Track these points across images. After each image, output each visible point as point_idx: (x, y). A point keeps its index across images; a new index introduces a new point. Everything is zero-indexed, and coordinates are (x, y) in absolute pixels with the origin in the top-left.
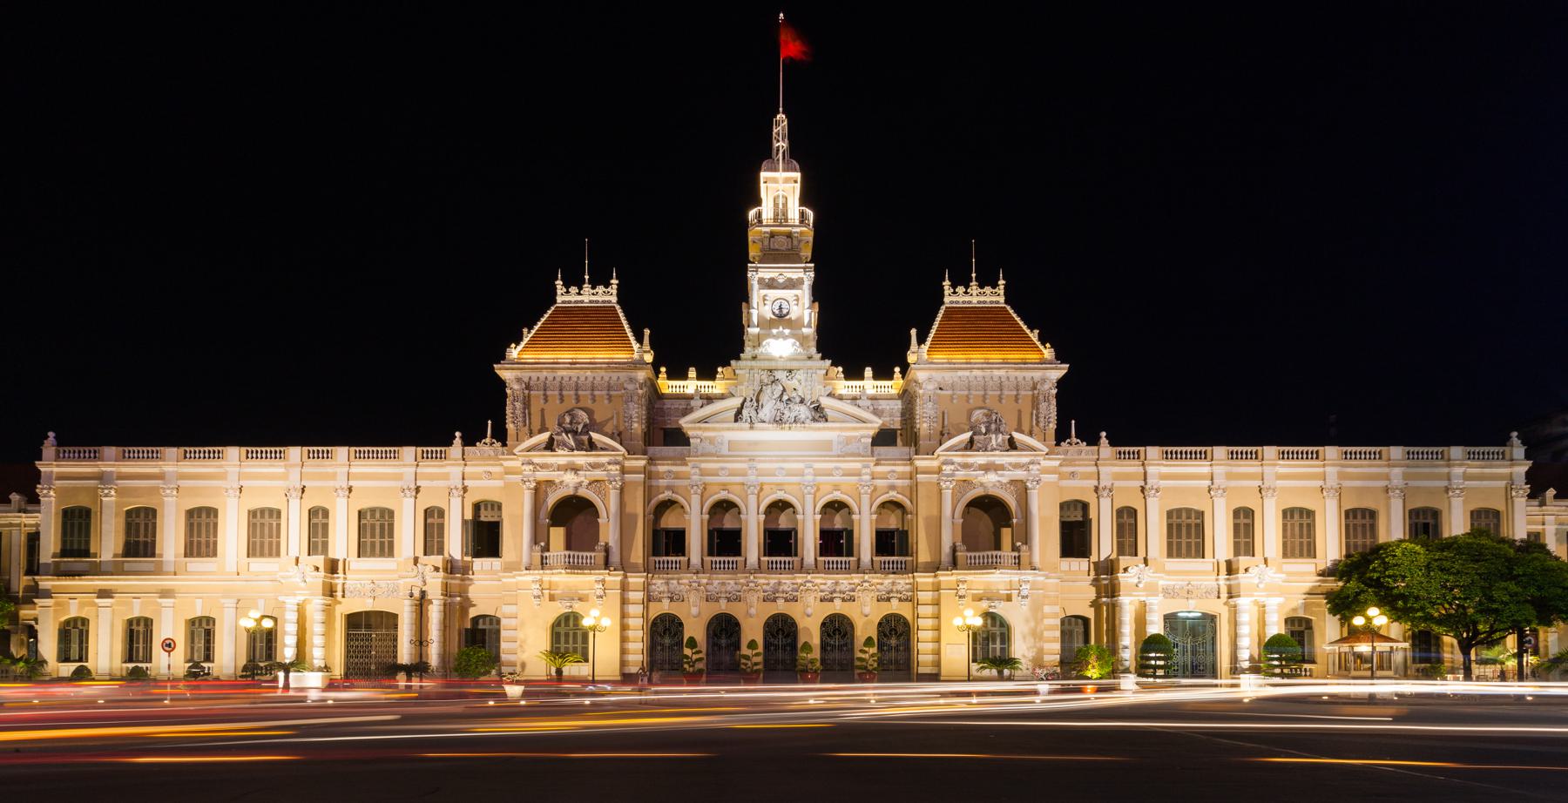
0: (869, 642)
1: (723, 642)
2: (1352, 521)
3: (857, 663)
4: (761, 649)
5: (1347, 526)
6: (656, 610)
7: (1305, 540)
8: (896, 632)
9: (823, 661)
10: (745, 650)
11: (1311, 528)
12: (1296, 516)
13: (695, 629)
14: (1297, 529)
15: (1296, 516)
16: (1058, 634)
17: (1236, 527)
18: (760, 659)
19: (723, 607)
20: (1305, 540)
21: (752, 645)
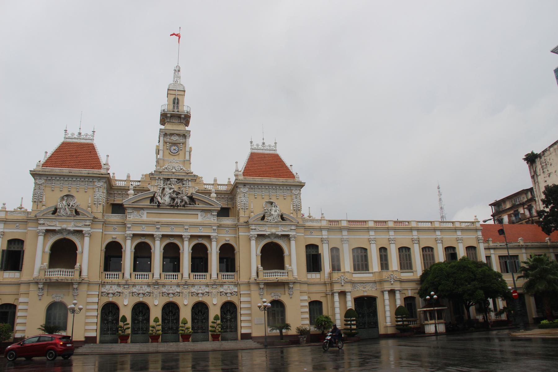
0: (216, 318)
1: (141, 318)
2: (425, 253)
3: (210, 329)
4: (160, 322)
5: (423, 255)
6: (105, 300)
7: (408, 262)
8: (229, 309)
9: (193, 328)
10: (152, 323)
11: (409, 257)
12: (404, 250)
13: (126, 312)
14: (405, 257)
15: (404, 250)
16: (307, 310)
17: (381, 256)
18: (160, 328)
19: (141, 299)
20: (408, 262)
21: (156, 320)
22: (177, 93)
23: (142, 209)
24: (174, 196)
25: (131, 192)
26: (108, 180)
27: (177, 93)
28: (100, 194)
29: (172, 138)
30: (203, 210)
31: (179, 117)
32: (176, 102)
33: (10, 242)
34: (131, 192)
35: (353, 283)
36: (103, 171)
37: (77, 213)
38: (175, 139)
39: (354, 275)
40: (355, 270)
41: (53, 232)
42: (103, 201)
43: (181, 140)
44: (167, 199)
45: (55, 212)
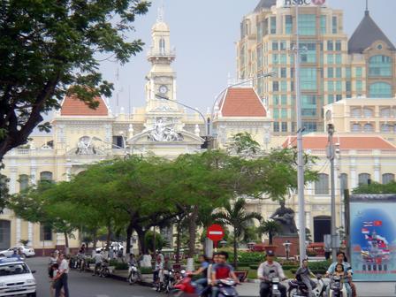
22: (162, 34)
23: (142, 145)
24: (166, 133)
25: (131, 130)
26: (115, 125)
27: (162, 34)
28: (109, 135)
29: (162, 79)
30: (189, 145)
31: (166, 58)
32: (162, 44)
33: (41, 173)
34: (131, 130)
35: (314, 205)
36: (110, 116)
37: (95, 152)
38: (163, 81)
39: (316, 198)
40: (316, 193)
41: (77, 166)
42: (111, 140)
43: (169, 81)
44: (161, 136)
45: (76, 153)
